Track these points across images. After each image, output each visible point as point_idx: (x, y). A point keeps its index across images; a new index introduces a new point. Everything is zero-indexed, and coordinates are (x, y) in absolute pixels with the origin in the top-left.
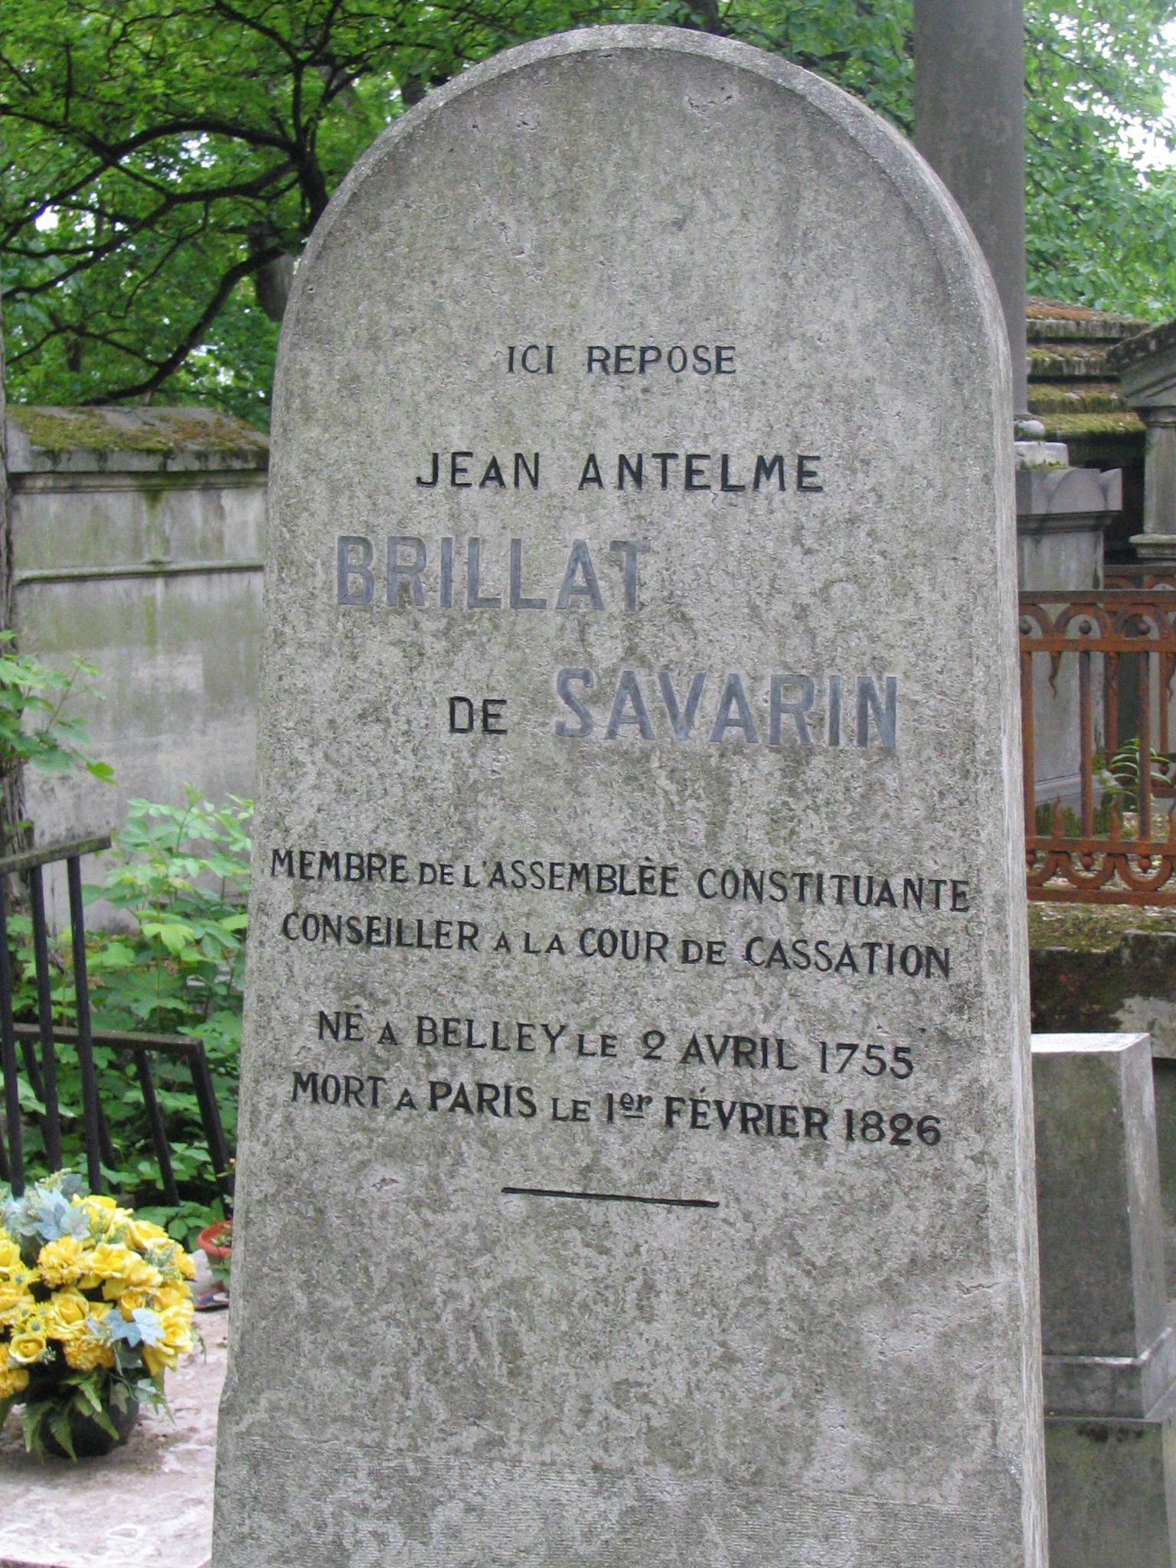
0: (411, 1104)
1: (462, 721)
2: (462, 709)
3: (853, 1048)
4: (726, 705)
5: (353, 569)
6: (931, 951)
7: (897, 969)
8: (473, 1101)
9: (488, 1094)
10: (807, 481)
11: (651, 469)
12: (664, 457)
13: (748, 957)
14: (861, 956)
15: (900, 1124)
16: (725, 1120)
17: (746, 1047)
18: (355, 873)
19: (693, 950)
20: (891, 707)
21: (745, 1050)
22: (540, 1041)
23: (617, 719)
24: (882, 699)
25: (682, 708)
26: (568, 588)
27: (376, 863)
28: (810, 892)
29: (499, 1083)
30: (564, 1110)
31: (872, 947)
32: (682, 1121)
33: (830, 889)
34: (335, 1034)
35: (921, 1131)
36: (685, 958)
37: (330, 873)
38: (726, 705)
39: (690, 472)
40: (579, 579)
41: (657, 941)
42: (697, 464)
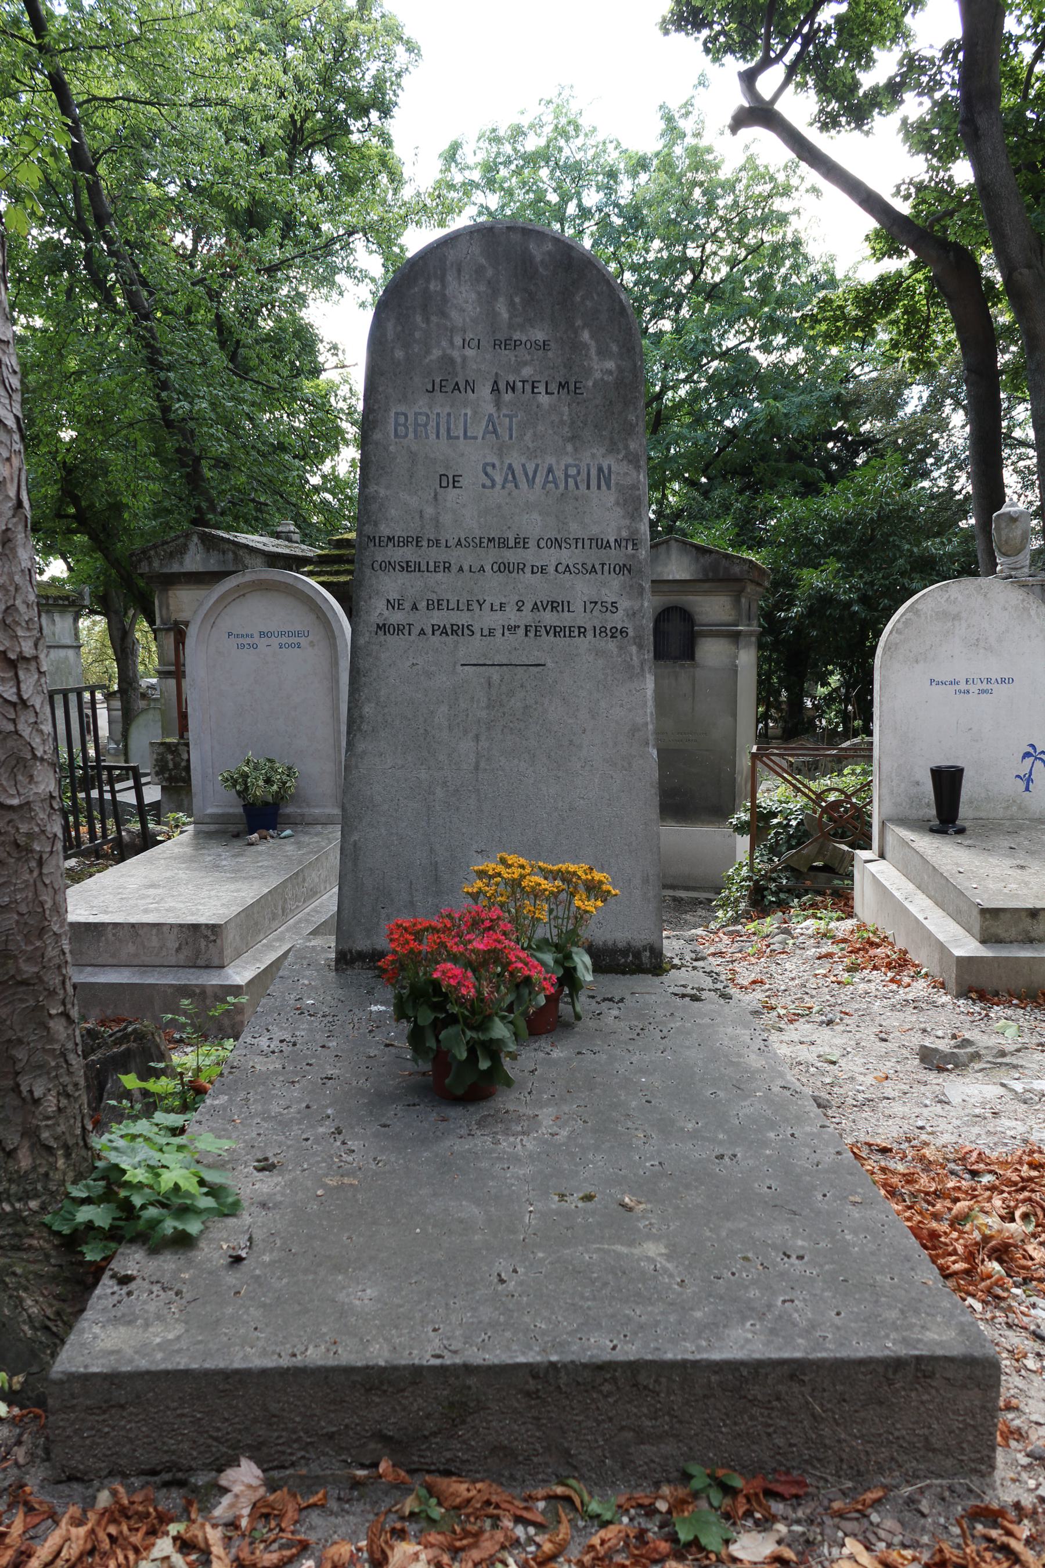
1: (444, 484)
2: (444, 478)
4: (547, 476)
14: (598, 567)
16: (548, 633)
21: (553, 606)
22: (476, 606)
23: (506, 480)
25: (531, 475)
28: (580, 545)
30: (486, 632)
31: (603, 565)
32: (531, 634)
33: (587, 543)
37: (391, 545)
38: (547, 476)
39: (533, 387)
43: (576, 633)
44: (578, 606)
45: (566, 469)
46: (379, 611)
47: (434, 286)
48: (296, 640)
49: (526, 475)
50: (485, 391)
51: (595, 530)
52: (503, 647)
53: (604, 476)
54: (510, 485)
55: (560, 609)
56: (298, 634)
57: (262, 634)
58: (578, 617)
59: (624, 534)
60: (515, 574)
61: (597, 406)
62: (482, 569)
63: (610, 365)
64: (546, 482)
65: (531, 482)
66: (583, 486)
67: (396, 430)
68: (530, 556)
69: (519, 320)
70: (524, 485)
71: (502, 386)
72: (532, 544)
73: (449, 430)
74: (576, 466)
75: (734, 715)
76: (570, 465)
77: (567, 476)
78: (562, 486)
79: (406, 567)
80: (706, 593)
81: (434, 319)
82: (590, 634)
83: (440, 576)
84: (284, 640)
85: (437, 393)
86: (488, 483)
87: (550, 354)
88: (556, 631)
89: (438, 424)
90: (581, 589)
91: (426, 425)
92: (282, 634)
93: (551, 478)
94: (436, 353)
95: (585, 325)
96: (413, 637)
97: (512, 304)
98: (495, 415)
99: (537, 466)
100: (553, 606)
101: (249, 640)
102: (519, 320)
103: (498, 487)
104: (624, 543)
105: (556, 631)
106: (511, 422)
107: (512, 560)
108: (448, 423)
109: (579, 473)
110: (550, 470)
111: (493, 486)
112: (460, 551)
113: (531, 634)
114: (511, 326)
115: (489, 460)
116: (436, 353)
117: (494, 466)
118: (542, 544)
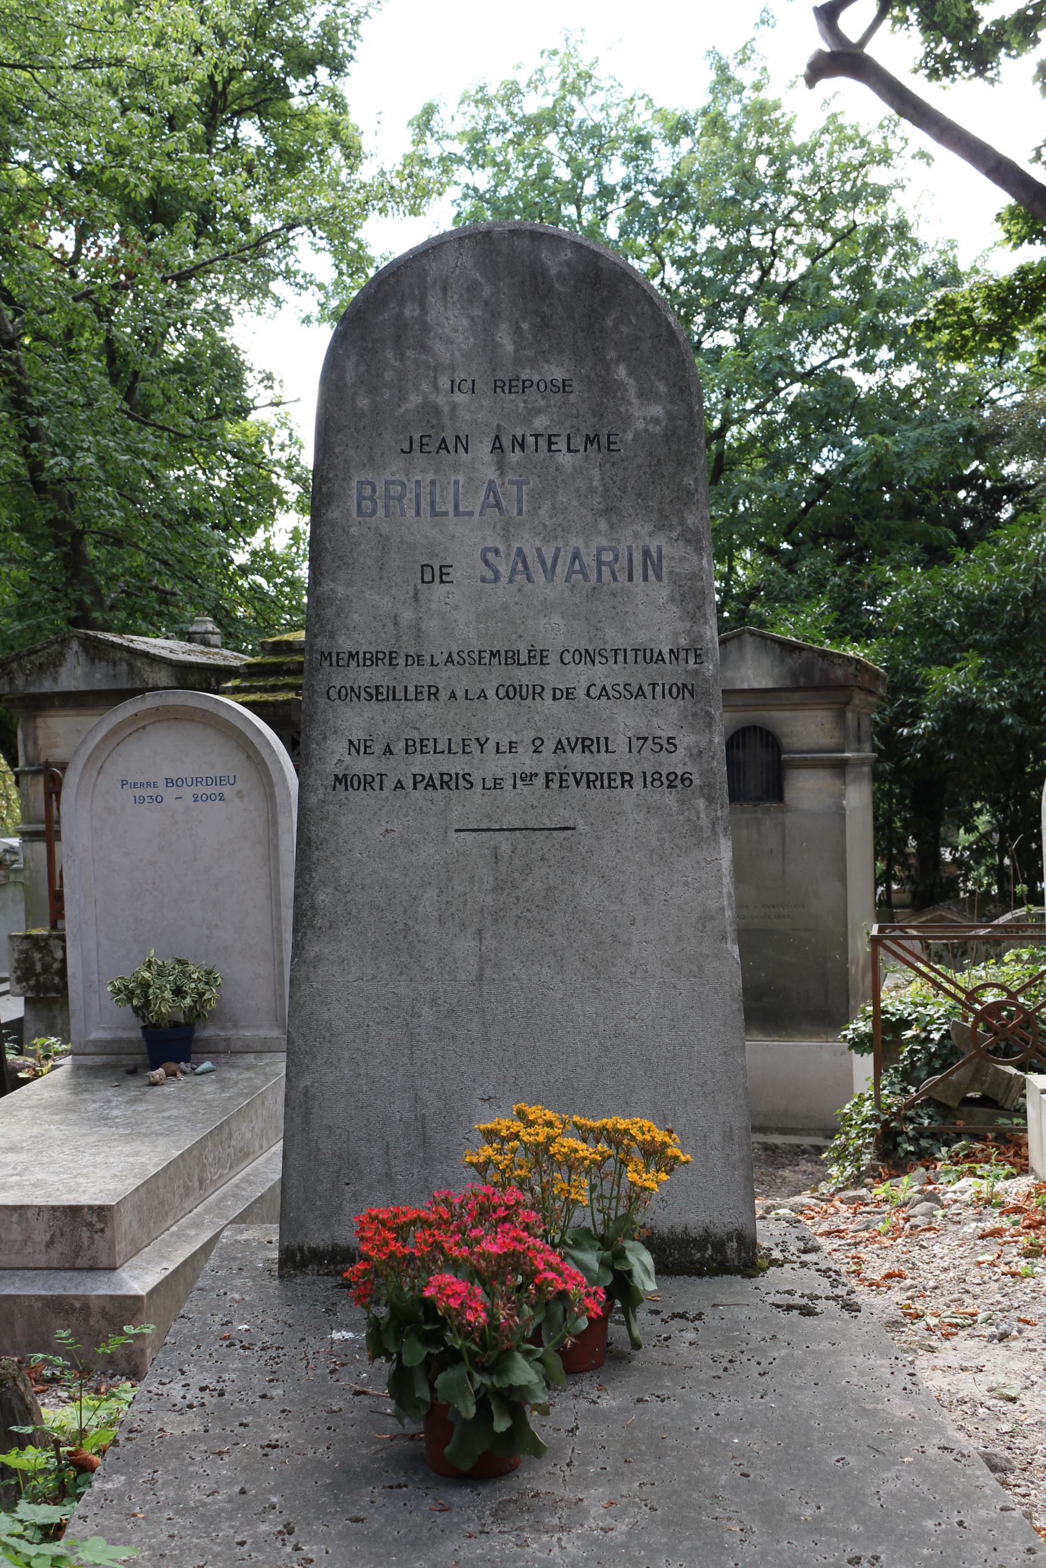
2: (428, 570)
3: (645, 739)
4: (572, 563)
8: (438, 783)
9: (446, 778)
12: (536, 436)
13: (588, 695)
14: (648, 690)
15: (672, 777)
16: (578, 783)
18: (368, 662)
21: (586, 744)
22: (474, 747)
24: (655, 556)
25: (549, 562)
27: (381, 656)
29: (453, 772)
30: (489, 784)
31: (654, 685)
32: (555, 785)
33: (631, 655)
34: (358, 752)
35: (683, 780)
36: (554, 698)
37: (353, 663)
38: (572, 563)
39: (550, 443)
41: (538, 690)
43: (619, 782)
44: (620, 744)
45: (599, 554)
46: (337, 757)
47: (410, 311)
48: (217, 789)
49: (543, 562)
50: (483, 449)
51: (641, 638)
52: (515, 805)
53: (652, 562)
54: (520, 578)
55: (594, 748)
56: (220, 781)
57: (169, 782)
58: (620, 759)
59: (683, 642)
60: (529, 701)
61: (639, 467)
62: (483, 694)
63: (657, 410)
64: (571, 572)
65: (550, 573)
66: (622, 577)
67: (359, 505)
68: (551, 675)
69: (529, 353)
70: (539, 577)
71: (507, 442)
72: (553, 658)
73: (433, 504)
74: (612, 549)
75: (843, 878)
76: (604, 549)
77: (600, 563)
78: (593, 578)
79: (375, 694)
80: (796, 706)
81: (411, 354)
82: (638, 783)
83: (423, 706)
84: (200, 790)
85: (416, 454)
86: (490, 575)
87: (572, 398)
88: (591, 780)
89: (418, 496)
90: (624, 720)
91: (400, 498)
92: (197, 781)
93: (577, 567)
94: (414, 400)
95: (621, 358)
96: (386, 792)
97: (518, 331)
98: (498, 482)
99: (558, 550)
100: (586, 744)
101: (151, 791)
102: (529, 353)
103: (504, 580)
104: (682, 655)
105: (591, 780)
106: (520, 490)
107: (525, 682)
108: (432, 494)
109: (616, 559)
110: (576, 556)
111: (497, 579)
112: (452, 670)
113: (555, 785)
114: (517, 362)
115: (489, 544)
116: (414, 400)
117: (497, 552)
118: (567, 657)
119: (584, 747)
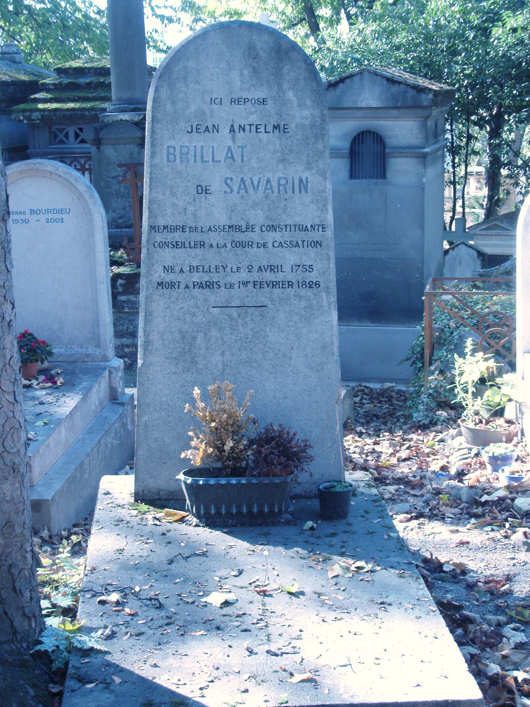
0: (188, 288)
1: (200, 191)
3: (299, 266)
4: (267, 185)
5: (170, 154)
6: (317, 242)
7: (309, 246)
8: (204, 286)
9: (208, 284)
10: (286, 131)
11: (247, 127)
12: (250, 125)
13: (273, 246)
14: (300, 243)
15: (311, 283)
16: (268, 285)
17: (273, 268)
18: (172, 230)
19: (260, 245)
20: (307, 184)
21: (272, 268)
23: (240, 188)
24: (305, 182)
25: (256, 184)
26: (227, 157)
27: (178, 227)
28: (288, 229)
29: (211, 281)
30: (228, 286)
31: (303, 241)
32: (258, 287)
33: (293, 228)
34: (168, 271)
35: (316, 284)
36: (258, 247)
38: (267, 185)
39: (257, 128)
40: (229, 155)
41: (250, 243)
42: (258, 127)
43: (287, 286)
44: (287, 268)
45: (279, 180)
46: (158, 274)
47: (191, 64)
48: (60, 216)
49: (253, 184)
50: (225, 130)
51: (298, 220)
52: (238, 296)
53: (303, 185)
54: (242, 191)
55: (276, 270)
56: (61, 211)
57: (32, 212)
58: (287, 275)
59: (317, 221)
60: (246, 249)
61: (298, 140)
62: (225, 246)
63: (306, 113)
64: (266, 189)
65: (256, 188)
66: (290, 192)
67: (168, 157)
68: (255, 236)
69: (247, 86)
70: (251, 191)
71: (236, 127)
72: (257, 229)
73: (202, 157)
74: (285, 178)
75: (422, 227)
76: (282, 178)
77: (279, 185)
78: (276, 191)
79: (176, 245)
80: (395, 118)
81: (191, 85)
82: (295, 285)
83: (197, 251)
84: (50, 216)
85: (194, 133)
86: (228, 190)
87: (267, 106)
88: (274, 284)
89: (195, 153)
90: (290, 258)
91: (187, 153)
92: (48, 211)
93: (269, 187)
94: (193, 108)
95: (290, 88)
96: (180, 290)
97: (242, 74)
98: (232, 147)
99: (260, 178)
100: (272, 268)
101: (22, 217)
102: (247, 86)
103: (235, 193)
104: (316, 228)
105: (274, 284)
106: (242, 151)
107: (244, 240)
108: (202, 152)
109: (287, 183)
110: (268, 181)
111: (232, 191)
112: (212, 234)
113: (258, 287)
114: (242, 90)
115: (228, 176)
116: (193, 108)
117: (232, 179)
118: (264, 229)
119: (271, 269)
